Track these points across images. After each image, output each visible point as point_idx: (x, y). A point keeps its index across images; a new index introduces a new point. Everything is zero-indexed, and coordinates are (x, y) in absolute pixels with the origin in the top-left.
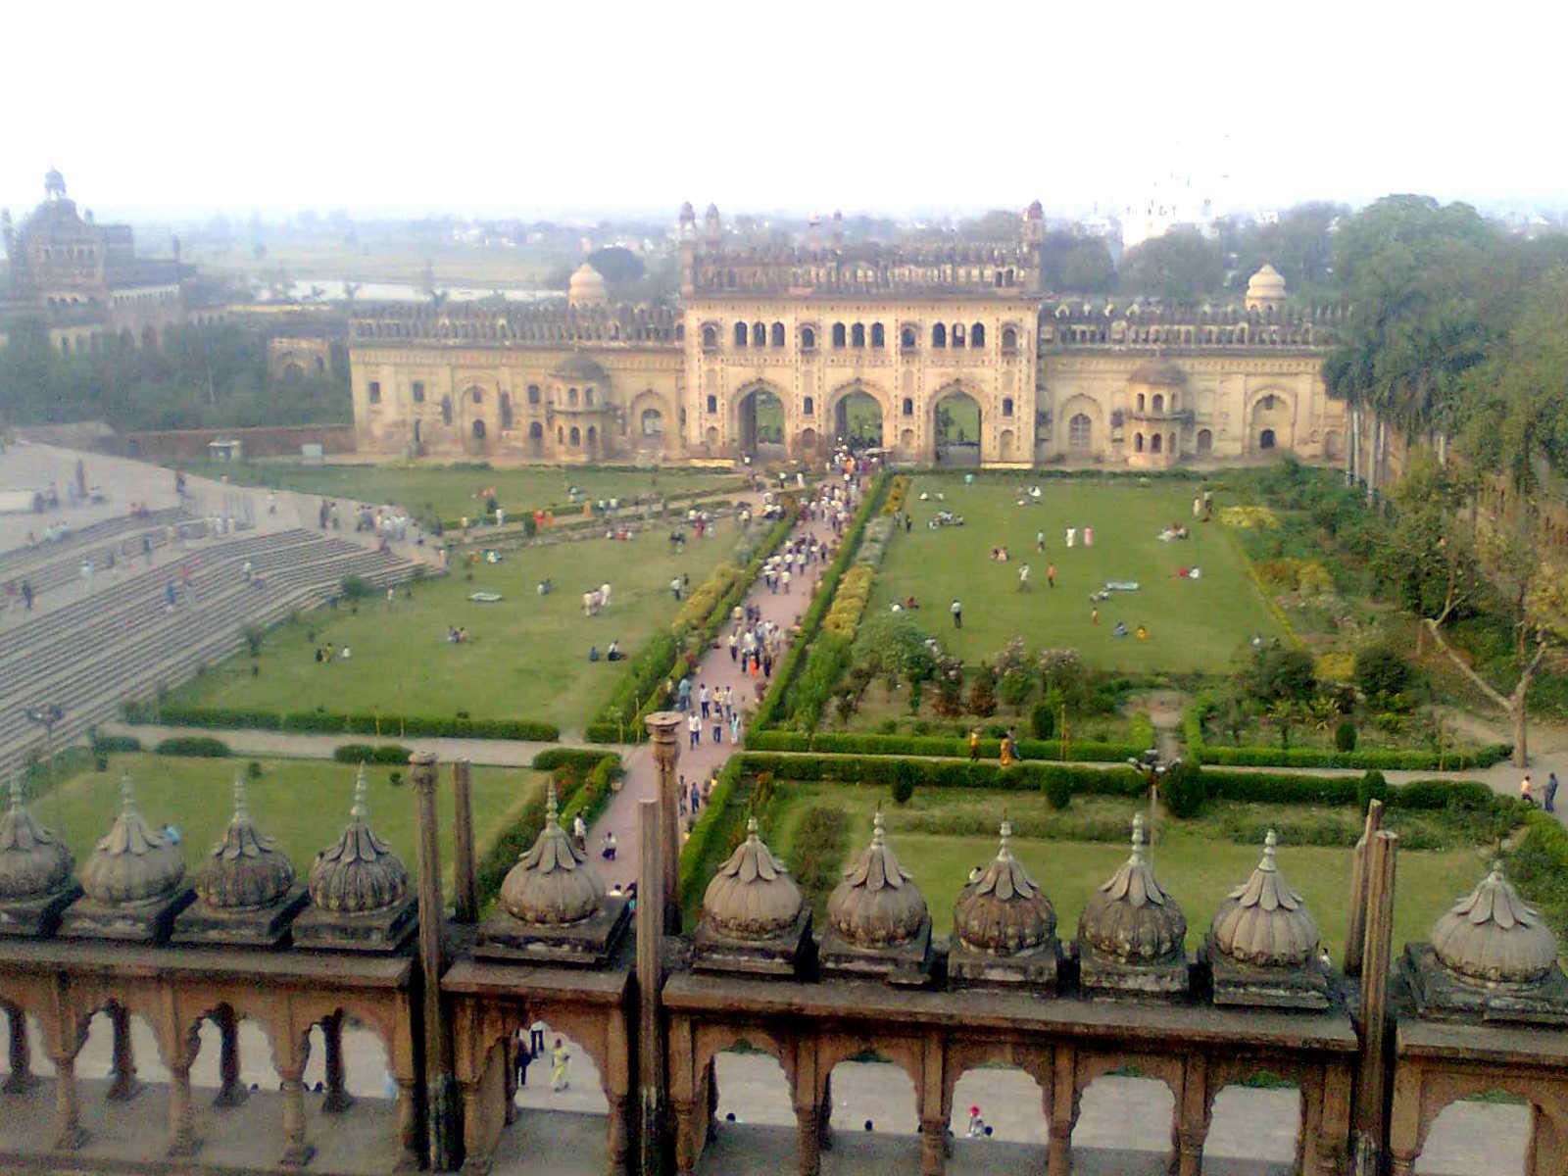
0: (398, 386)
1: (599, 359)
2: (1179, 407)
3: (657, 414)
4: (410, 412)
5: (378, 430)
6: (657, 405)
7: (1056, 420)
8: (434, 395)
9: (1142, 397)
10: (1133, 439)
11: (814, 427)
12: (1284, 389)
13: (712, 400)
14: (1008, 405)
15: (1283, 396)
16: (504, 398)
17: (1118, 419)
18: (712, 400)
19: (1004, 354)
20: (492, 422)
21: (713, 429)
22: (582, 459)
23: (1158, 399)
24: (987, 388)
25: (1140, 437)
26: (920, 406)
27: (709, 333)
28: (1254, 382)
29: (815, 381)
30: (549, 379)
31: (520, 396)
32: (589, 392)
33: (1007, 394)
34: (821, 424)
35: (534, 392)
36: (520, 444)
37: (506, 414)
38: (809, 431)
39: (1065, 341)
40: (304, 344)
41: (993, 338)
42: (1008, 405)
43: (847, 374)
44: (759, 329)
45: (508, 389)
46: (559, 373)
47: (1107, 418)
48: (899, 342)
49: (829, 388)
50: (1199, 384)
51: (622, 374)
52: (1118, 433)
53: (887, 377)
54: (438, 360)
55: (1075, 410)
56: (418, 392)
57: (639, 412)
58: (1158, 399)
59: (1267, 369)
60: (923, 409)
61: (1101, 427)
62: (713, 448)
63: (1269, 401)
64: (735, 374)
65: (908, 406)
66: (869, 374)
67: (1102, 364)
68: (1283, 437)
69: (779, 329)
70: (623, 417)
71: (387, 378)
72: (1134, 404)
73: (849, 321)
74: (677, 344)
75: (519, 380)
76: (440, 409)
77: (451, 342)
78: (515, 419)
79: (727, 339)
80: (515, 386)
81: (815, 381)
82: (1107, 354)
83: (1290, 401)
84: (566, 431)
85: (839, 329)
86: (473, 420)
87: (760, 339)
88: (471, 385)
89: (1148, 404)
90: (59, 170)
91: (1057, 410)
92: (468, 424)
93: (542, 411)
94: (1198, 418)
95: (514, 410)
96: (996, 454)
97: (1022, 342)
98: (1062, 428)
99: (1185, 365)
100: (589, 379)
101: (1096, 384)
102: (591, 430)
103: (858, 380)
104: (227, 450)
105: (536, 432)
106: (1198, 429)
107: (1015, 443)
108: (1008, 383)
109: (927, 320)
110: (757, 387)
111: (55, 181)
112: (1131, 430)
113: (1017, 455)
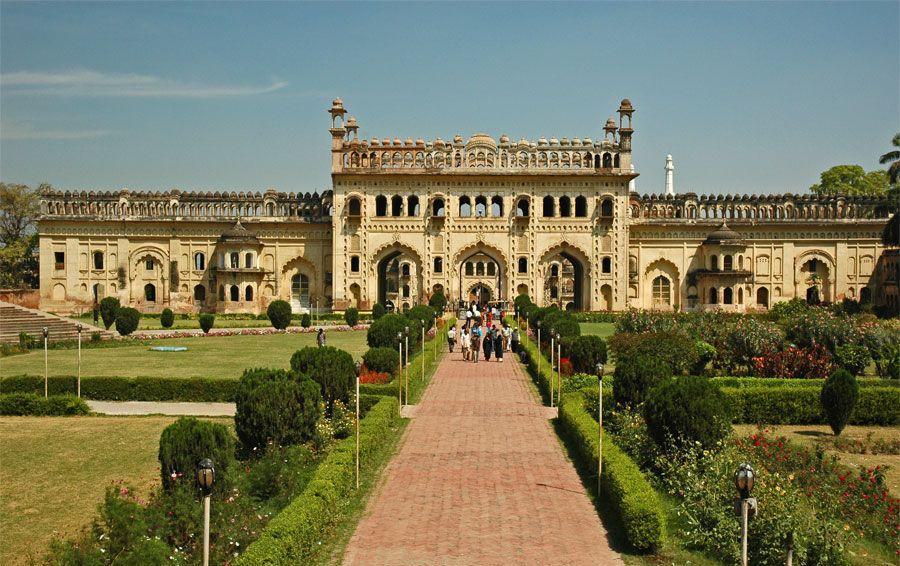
2: (746, 266)
5: (58, 294)
6: (305, 271)
7: (641, 282)
8: (109, 263)
9: (714, 259)
13: (355, 262)
14: (606, 263)
15: (824, 260)
16: (174, 265)
23: (728, 260)
27: (354, 205)
29: (445, 243)
32: (249, 257)
33: (607, 254)
36: (183, 304)
37: (174, 279)
42: (606, 263)
51: (277, 244)
52: (692, 291)
55: (657, 273)
56: (98, 259)
63: (812, 266)
65: (523, 265)
72: (708, 266)
76: (116, 275)
78: (181, 283)
81: (445, 243)
86: (147, 283)
87: (397, 212)
88: (145, 254)
91: (642, 270)
94: (756, 279)
95: (181, 276)
106: (757, 287)
108: (607, 246)
110: (394, 250)
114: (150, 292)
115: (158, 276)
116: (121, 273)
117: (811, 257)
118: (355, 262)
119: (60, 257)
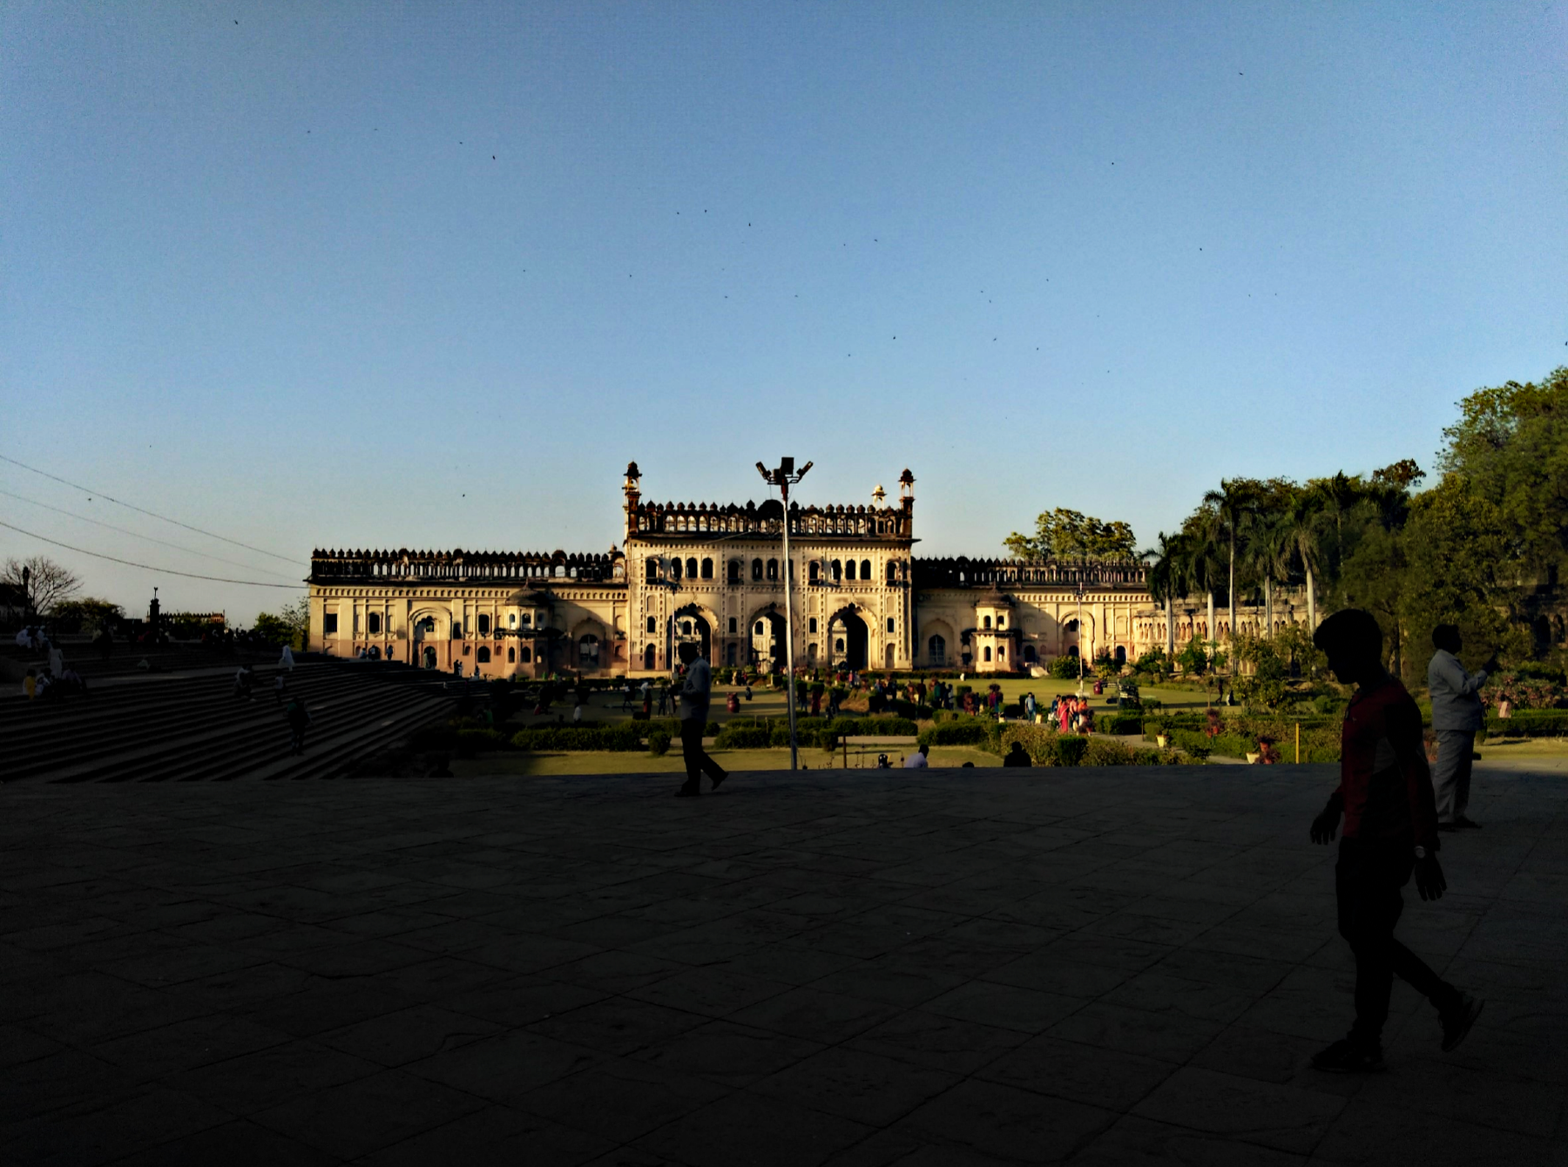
0: (356, 617)
3: (593, 639)
9: (987, 619)
13: (651, 623)
19: (889, 584)
21: (651, 647)
31: (472, 625)
41: (878, 572)
42: (891, 622)
44: (692, 563)
47: (958, 637)
52: (966, 649)
57: (578, 637)
58: (1000, 620)
60: (826, 627)
61: (955, 647)
67: (951, 595)
71: (343, 608)
72: (981, 625)
75: (472, 611)
80: (466, 618)
87: (692, 574)
88: (425, 616)
97: (898, 575)
101: (949, 611)
117: (1072, 618)
118: (651, 623)
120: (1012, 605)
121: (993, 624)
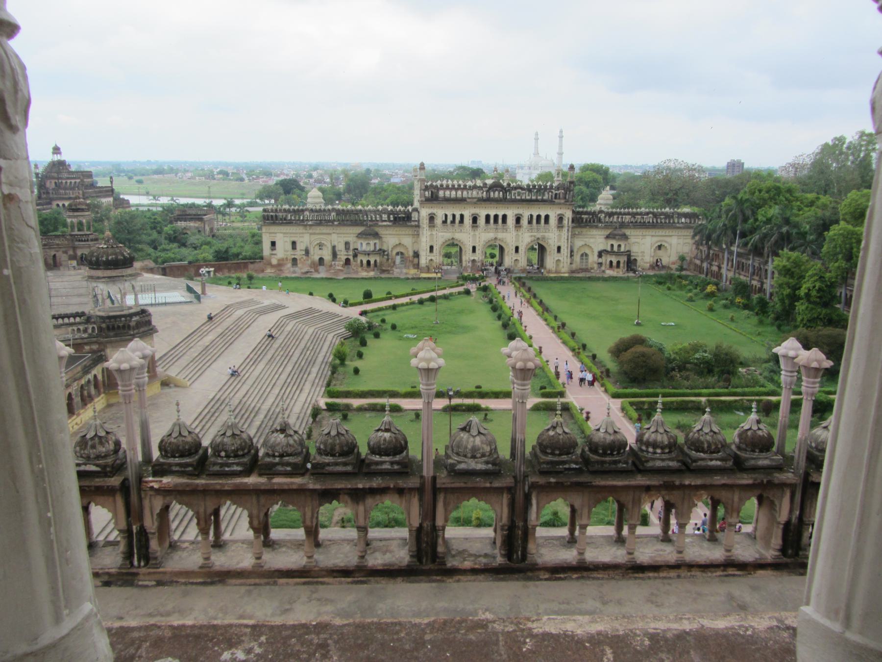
1: (377, 229)
3: (402, 253)
4: (290, 254)
5: (274, 262)
8: (300, 247)
9: (612, 246)
10: (608, 263)
11: (476, 258)
12: (666, 242)
13: (431, 248)
14: (559, 249)
15: (666, 245)
16: (334, 247)
17: (600, 255)
18: (431, 248)
19: (558, 227)
20: (327, 257)
22: (372, 274)
23: (619, 246)
24: (551, 242)
25: (611, 262)
26: (522, 249)
27: (432, 218)
28: (655, 239)
30: (355, 239)
31: (341, 247)
33: (559, 244)
34: (478, 256)
35: (347, 244)
37: (335, 255)
38: (474, 261)
39: (583, 221)
40: (192, 224)
41: (553, 221)
42: (559, 249)
43: (491, 235)
44: (454, 216)
45: (336, 244)
46: (360, 236)
47: (596, 254)
48: (514, 222)
49: (482, 243)
50: (632, 240)
52: (600, 260)
53: (509, 237)
54: (304, 231)
56: (294, 244)
57: (394, 253)
58: (619, 246)
59: (660, 234)
62: (431, 268)
63: (660, 247)
64: (441, 236)
65: (517, 249)
66: (500, 235)
67: (594, 232)
68: (665, 261)
69: (462, 216)
70: (388, 255)
72: (609, 249)
73: (492, 213)
74: (413, 223)
77: (310, 223)
79: (439, 221)
82: (597, 227)
83: (668, 247)
84: (365, 262)
85: (488, 217)
87: (453, 221)
89: (615, 249)
90: (59, 145)
91: (575, 250)
92: (317, 258)
93: (351, 253)
95: (338, 253)
96: (554, 269)
97: (565, 222)
98: (577, 258)
99: (628, 232)
100: (376, 239)
101: (592, 240)
102: (375, 261)
103: (496, 238)
104: (209, 272)
105: (347, 262)
107: (561, 265)
109: (526, 212)
111: (57, 150)
112: (607, 259)
113: (563, 270)
114: (321, 260)
115: (327, 256)
116: (307, 252)
119: (273, 244)
120: (625, 237)
121: (615, 249)
